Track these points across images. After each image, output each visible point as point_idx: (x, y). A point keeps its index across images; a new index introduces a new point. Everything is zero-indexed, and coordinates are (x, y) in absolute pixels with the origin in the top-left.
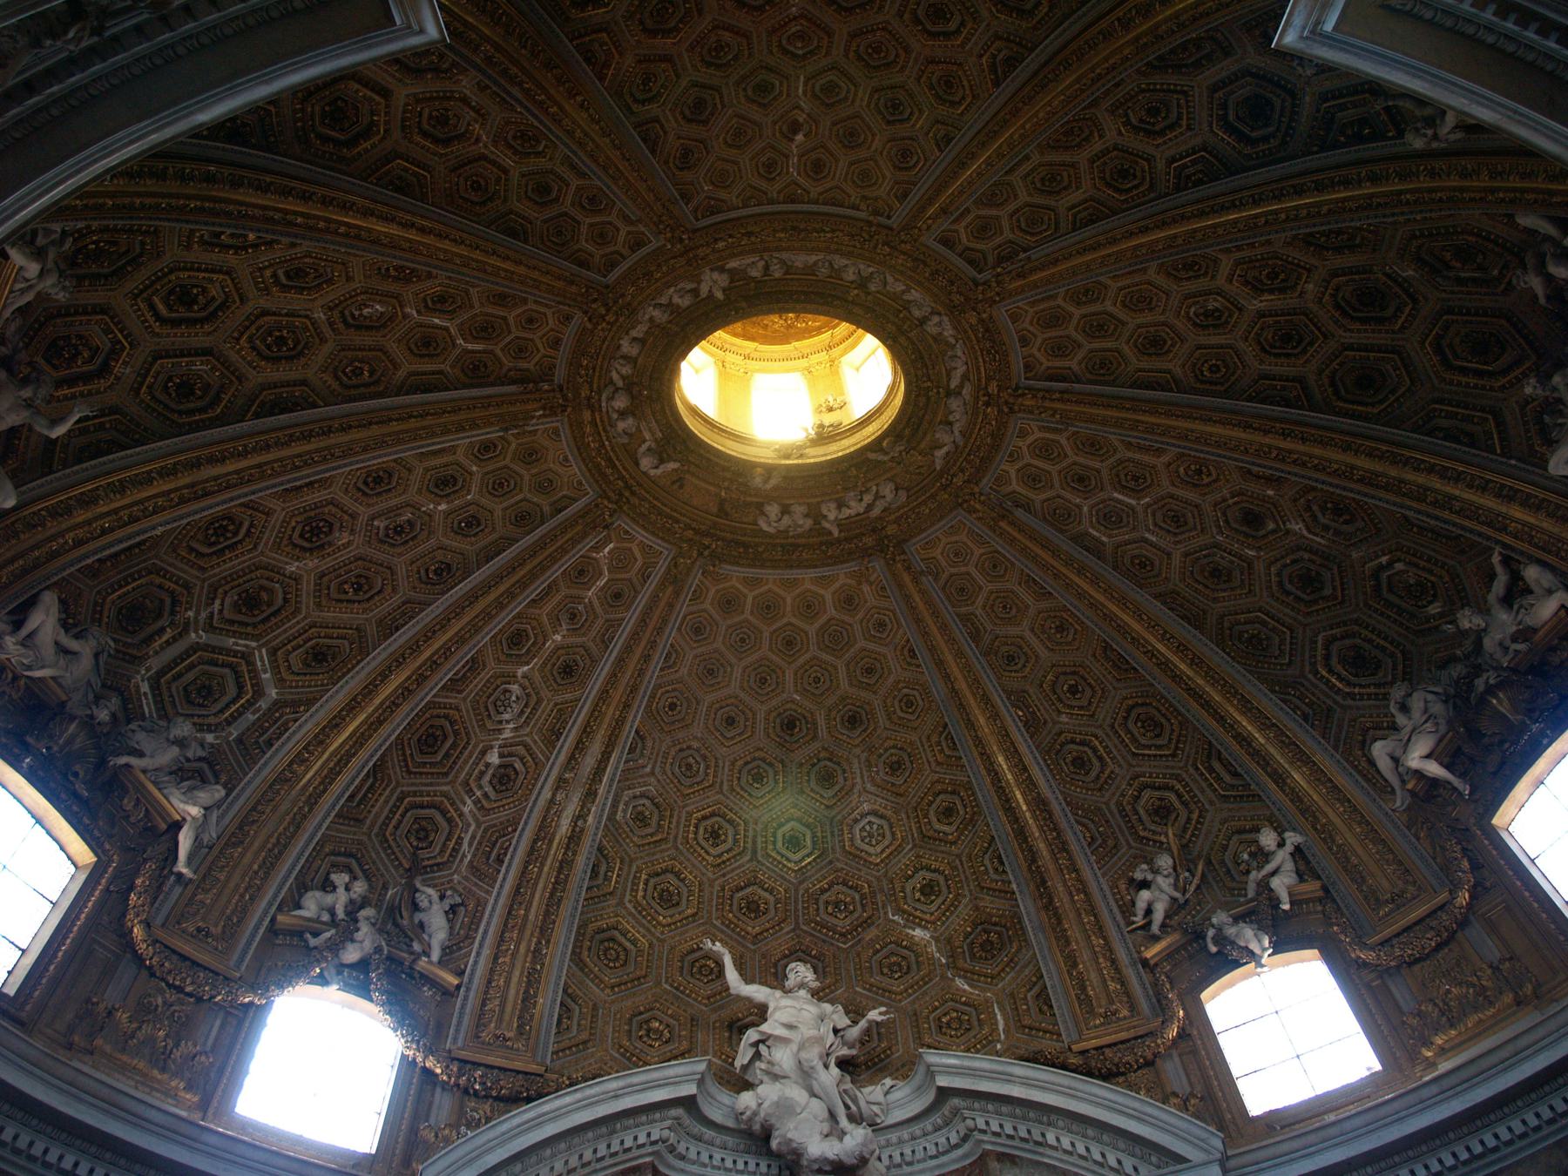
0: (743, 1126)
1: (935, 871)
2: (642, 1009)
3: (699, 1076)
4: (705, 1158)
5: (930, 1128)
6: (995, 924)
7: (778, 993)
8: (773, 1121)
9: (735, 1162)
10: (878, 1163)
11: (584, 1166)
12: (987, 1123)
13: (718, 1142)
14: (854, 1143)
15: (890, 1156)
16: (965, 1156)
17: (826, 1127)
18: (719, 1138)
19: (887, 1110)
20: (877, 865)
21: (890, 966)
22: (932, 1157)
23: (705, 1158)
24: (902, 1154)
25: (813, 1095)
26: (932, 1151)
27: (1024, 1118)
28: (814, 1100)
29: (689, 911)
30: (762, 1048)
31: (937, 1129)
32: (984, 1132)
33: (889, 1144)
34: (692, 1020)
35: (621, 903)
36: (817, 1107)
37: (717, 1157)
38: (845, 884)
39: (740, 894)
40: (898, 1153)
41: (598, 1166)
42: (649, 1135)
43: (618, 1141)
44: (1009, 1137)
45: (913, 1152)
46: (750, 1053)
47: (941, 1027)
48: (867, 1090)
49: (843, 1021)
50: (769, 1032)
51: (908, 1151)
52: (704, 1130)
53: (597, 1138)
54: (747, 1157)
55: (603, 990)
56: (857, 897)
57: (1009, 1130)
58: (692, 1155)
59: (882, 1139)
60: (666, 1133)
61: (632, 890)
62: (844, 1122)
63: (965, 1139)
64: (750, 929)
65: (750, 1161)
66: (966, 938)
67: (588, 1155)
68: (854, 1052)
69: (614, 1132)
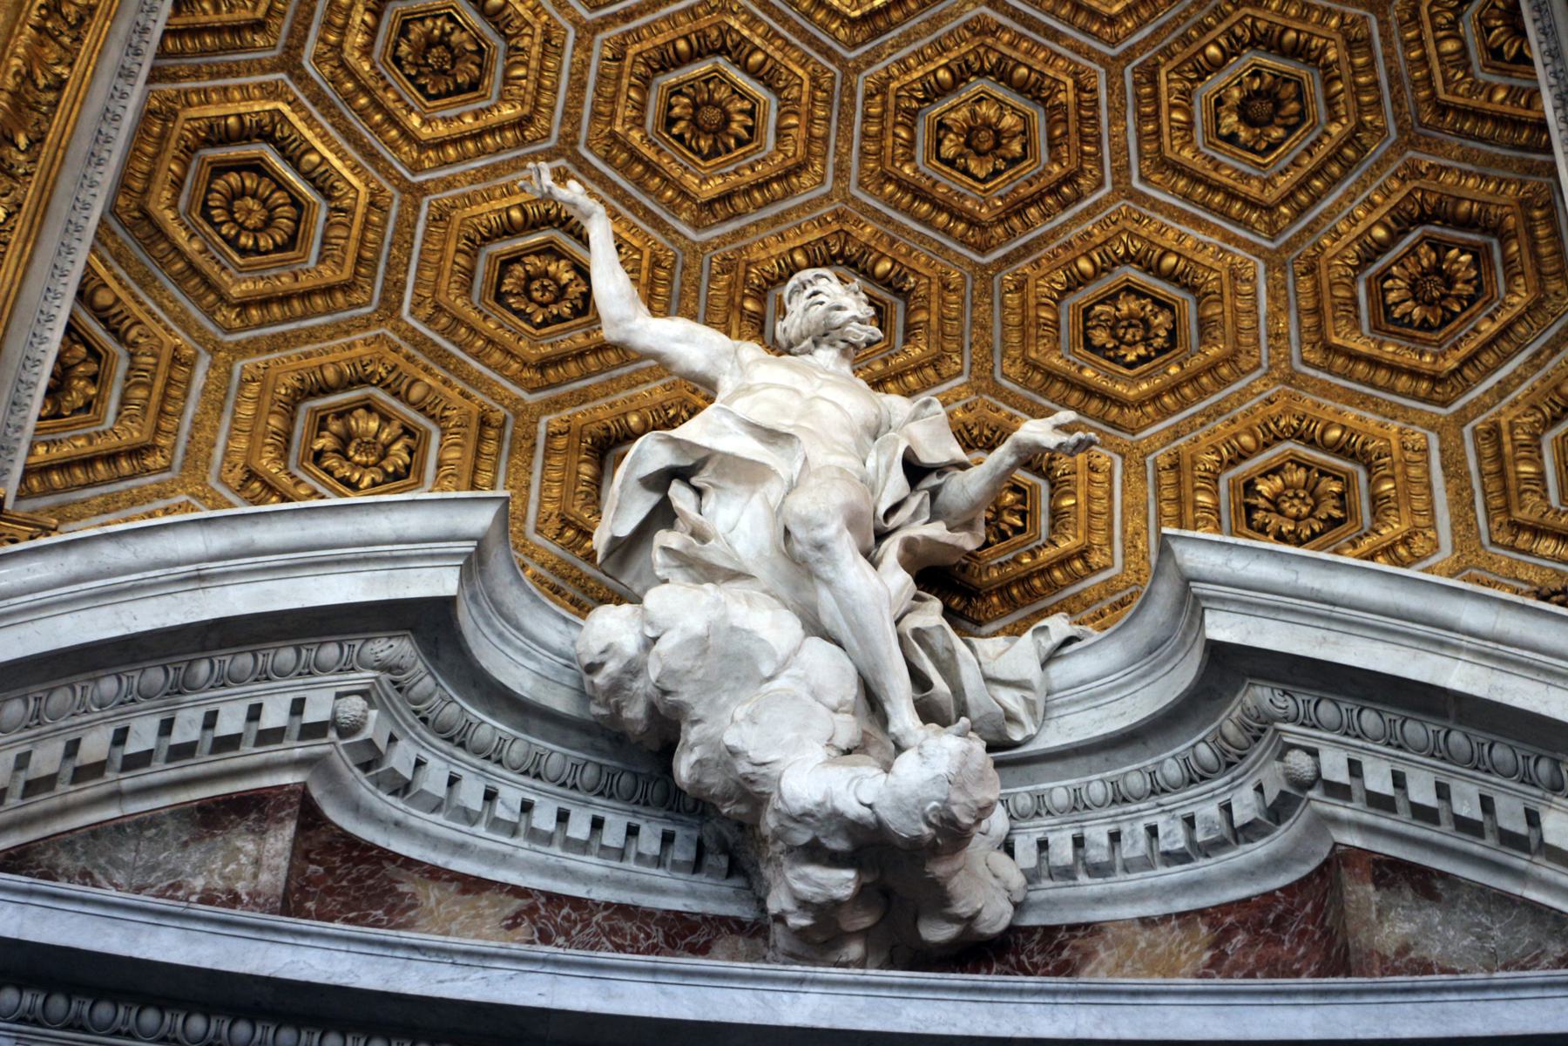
0: (596, 710)
1: (1297, 52)
2: (330, 374)
3: (468, 547)
4: (471, 794)
5: (1173, 771)
6: (1468, 223)
7: (751, 351)
8: (686, 694)
9: (563, 817)
10: (1001, 858)
11: (82, 774)
12: (1355, 768)
13: (516, 752)
14: (927, 773)
15: (1043, 845)
16: (1276, 863)
17: (847, 729)
18: (521, 745)
19: (1045, 709)
20: (1112, 20)
21: (1113, 326)
22: (1172, 858)
23: (471, 794)
24: (1079, 842)
25: (815, 627)
26: (1174, 837)
27: (1476, 763)
28: (817, 645)
29: (507, 112)
30: (680, 496)
31: (1196, 776)
32: (1338, 791)
33: (1041, 807)
34: (484, 422)
35: (290, 62)
36: (821, 660)
37: (511, 797)
38: (1002, 74)
39: (672, 78)
40: (1067, 835)
41: (128, 782)
42: (298, 707)
43: (198, 715)
44: (1422, 813)
45: (1115, 837)
46: (640, 506)
47: (1251, 509)
48: (989, 646)
49: (939, 447)
50: (705, 441)
51: (1097, 834)
52: (476, 713)
53: (127, 700)
54: (601, 806)
55: (210, 313)
57: (1421, 791)
58: (434, 781)
59: (1023, 796)
60: (357, 703)
61: (328, 24)
62: (904, 717)
63: (1279, 811)
64: (691, 181)
65: (609, 818)
66: (1365, 260)
67: (96, 745)
68: (967, 542)
69: (181, 687)
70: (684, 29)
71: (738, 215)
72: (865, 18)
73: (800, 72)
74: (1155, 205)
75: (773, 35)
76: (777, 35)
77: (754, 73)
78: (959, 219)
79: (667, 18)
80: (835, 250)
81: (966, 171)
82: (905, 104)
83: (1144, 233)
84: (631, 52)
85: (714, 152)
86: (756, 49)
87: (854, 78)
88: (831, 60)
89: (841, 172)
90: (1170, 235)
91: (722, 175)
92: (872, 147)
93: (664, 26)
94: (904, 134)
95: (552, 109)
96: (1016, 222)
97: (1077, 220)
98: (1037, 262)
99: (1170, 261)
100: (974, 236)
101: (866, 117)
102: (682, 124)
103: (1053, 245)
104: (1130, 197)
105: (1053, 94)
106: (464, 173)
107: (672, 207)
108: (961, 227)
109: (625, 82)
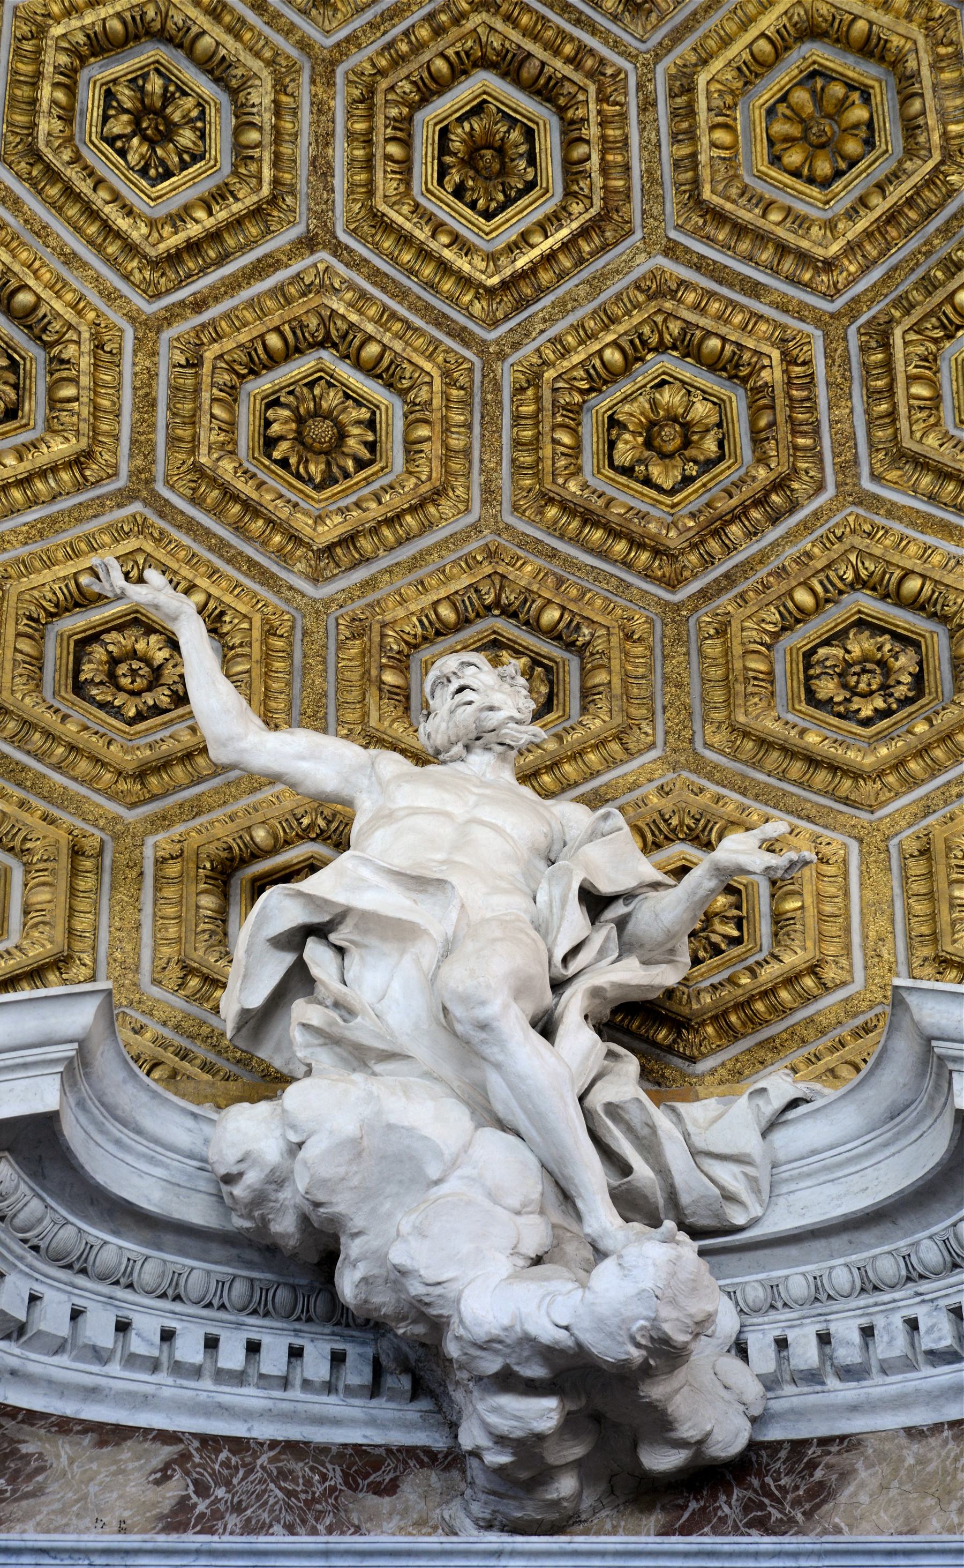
29: (59, 448)
39: (265, 384)
56: (738, 402)
64: (302, 523)
70: (275, 320)
71: (365, 560)
72: (505, 285)
73: (428, 366)
74: (892, 511)
75: (387, 317)
76: (394, 316)
77: (370, 370)
78: (642, 546)
79: (250, 304)
80: (489, 599)
81: (647, 481)
82: (564, 399)
83: (877, 551)
84: (209, 355)
85: (329, 480)
86: (370, 338)
87: (498, 366)
88: (466, 344)
89: (490, 494)
90: (912, 549)
91: (340, 511)
92: (527, 459)
93: (248, 315)
94: (566, 439)
95: (117, 438)
96: (714, 545)
97: (790, 537)
98: (742, 596)
99: (913, 585)
100: (661, 568)
101: (517, 418)
102: (284, 446)
103: (762, 572)
104: (860, 503)
105: (755, 370)
106: (13, 531)
107: (282, 556)
108: (645, 556)
109: (205, 396)
